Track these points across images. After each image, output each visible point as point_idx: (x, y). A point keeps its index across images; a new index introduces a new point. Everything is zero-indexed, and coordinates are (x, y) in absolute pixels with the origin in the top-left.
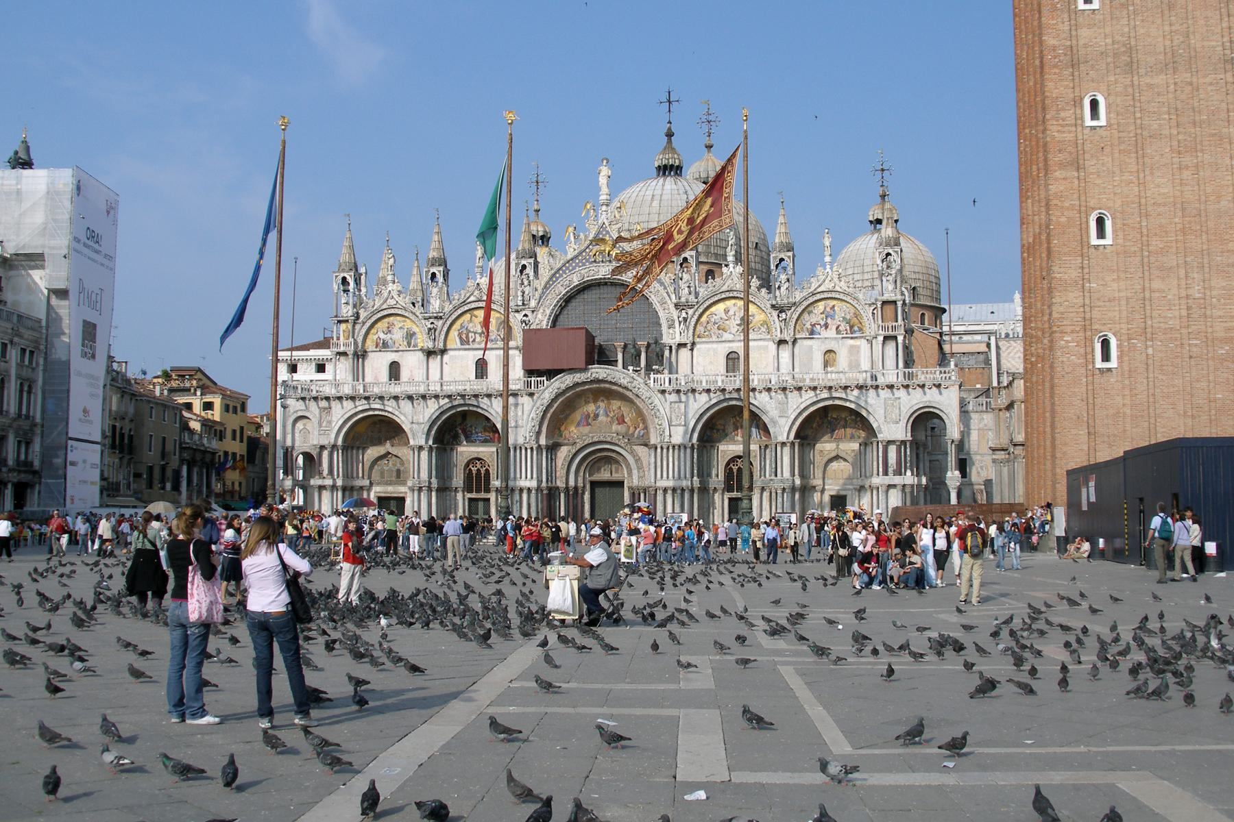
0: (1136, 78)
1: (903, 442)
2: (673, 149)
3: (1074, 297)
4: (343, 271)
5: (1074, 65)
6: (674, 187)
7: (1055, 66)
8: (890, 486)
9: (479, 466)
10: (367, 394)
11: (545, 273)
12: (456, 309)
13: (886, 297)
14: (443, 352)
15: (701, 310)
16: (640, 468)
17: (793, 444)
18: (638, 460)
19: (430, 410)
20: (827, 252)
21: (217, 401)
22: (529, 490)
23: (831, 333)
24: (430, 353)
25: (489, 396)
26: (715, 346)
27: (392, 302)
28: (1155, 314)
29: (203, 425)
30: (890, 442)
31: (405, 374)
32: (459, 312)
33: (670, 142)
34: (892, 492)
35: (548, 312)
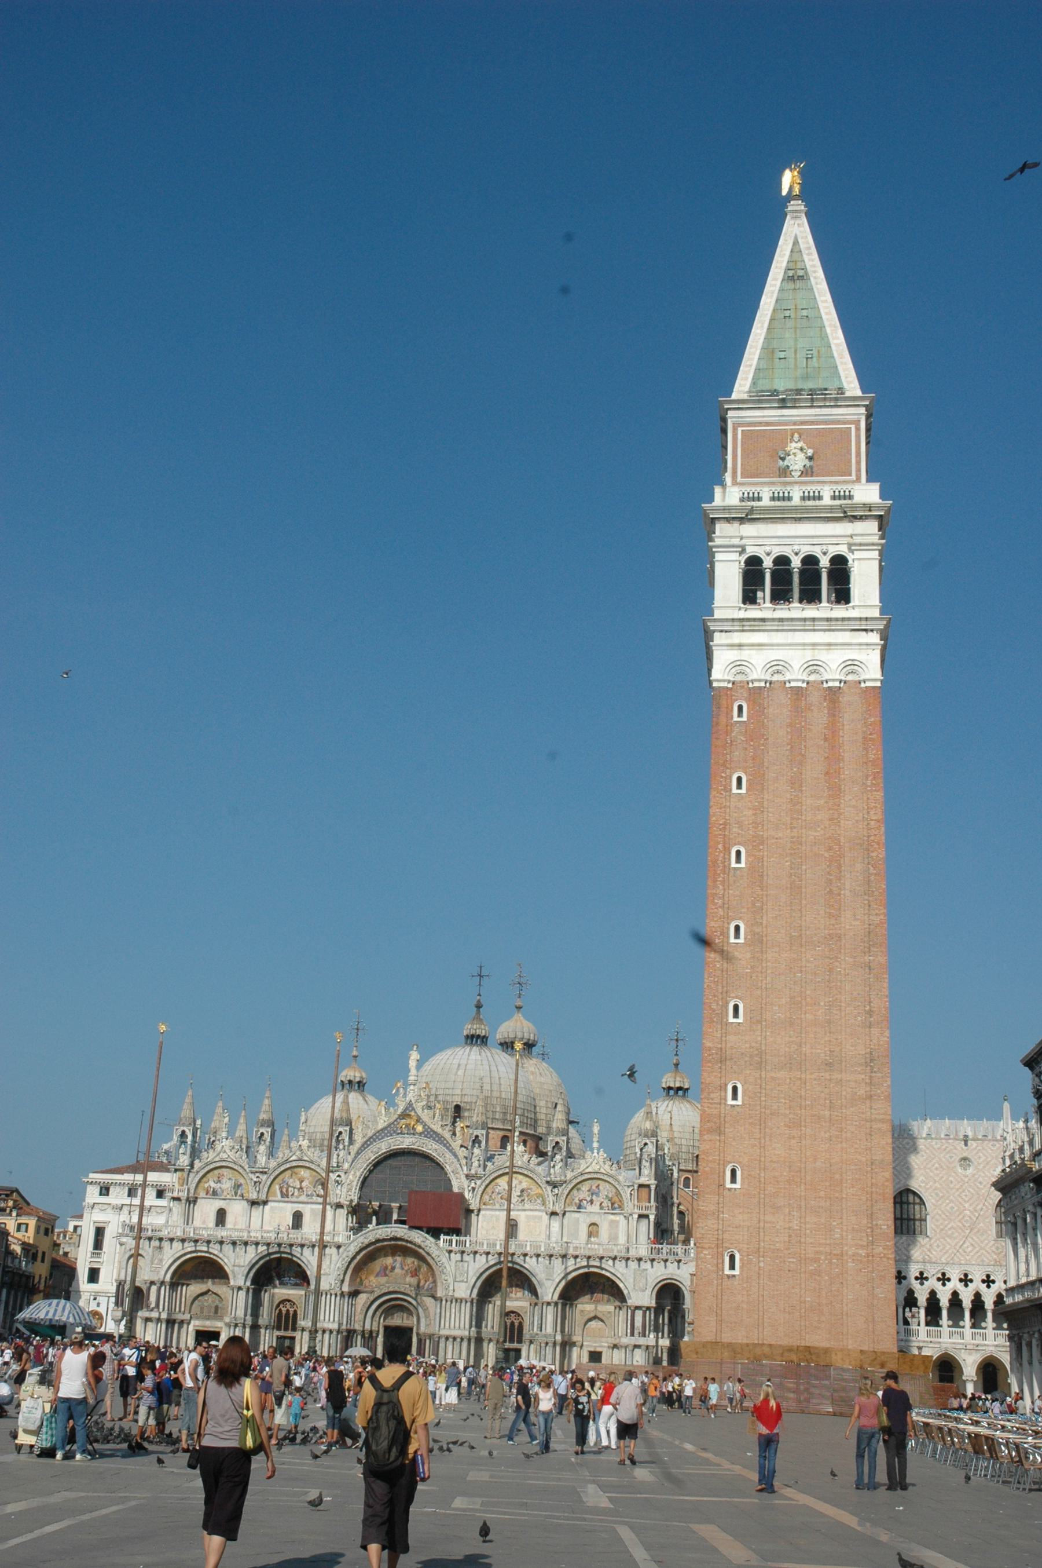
0: (763, 1073)
1: (648, 1308)
2: (481, 1020)
3: (711, 1223)
4: (183, 1125)
5: (722, 1061)
6: (479, 1057)
7: (709, 1062)
8: (636, 1346)
9: (288, 1306)
10: (197, 1237)
11: (359, 1140)
12: (279, 1165)
13: (643, 1180)
14: (265, 1203)
15: (487, 1182)
16: (427, 1317)
17: (556, 1304)
18: (426, 1310)
19: (250, 1255)
20: (595, 1139)
21: (32, 1223)
22: (331, 1332)
23: (595, 1208)
24: (254, 1203)
25: (302, 1246)
26: (497, 1213)
27: (225, 1156)
28: (767, 1238)
29: (23, 1249)
30: (637, 1308)
31: (230, 1219)
32: (282, 1168)
33: (478, 1013)
34: (636, 1350)
35: (358, 1174)
